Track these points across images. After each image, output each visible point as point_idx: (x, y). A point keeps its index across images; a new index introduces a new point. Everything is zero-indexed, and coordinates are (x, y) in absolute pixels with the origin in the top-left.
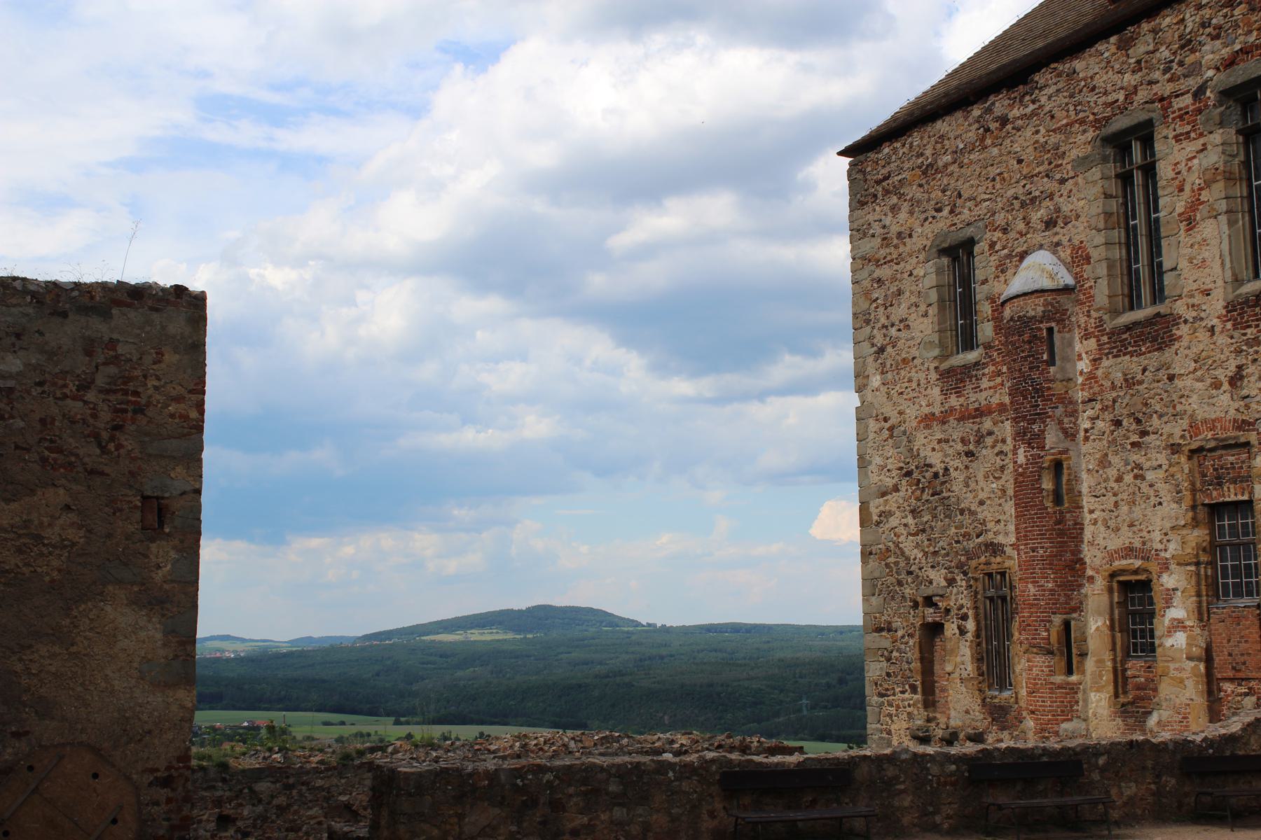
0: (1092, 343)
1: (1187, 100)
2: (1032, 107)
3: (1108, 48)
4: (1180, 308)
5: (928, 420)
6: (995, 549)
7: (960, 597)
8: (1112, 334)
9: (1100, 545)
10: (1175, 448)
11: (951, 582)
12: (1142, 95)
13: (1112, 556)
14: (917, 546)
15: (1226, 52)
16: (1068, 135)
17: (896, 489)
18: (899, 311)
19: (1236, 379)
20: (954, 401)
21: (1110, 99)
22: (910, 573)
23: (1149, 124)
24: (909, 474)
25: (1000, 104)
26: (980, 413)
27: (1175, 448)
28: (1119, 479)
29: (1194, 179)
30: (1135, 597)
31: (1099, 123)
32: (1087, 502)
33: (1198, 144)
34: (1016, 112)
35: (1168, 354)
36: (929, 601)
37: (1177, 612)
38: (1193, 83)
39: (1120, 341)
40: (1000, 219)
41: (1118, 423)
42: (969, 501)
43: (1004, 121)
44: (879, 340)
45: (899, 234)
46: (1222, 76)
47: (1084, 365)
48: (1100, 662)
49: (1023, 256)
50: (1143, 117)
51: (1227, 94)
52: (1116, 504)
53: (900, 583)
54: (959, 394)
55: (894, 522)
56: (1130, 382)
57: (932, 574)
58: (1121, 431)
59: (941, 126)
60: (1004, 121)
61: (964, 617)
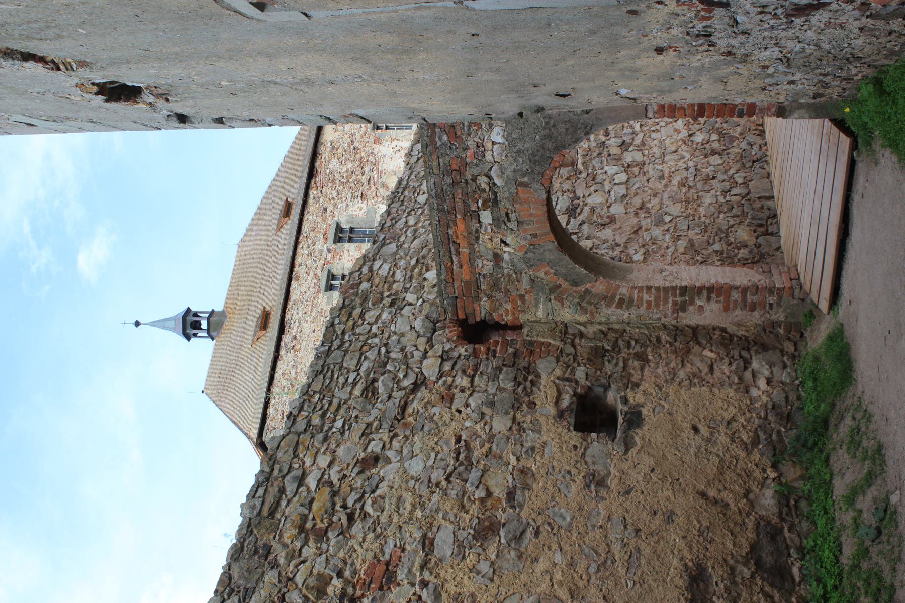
1: (329, 255)
2: (297, 324)
3: (294, 284)
12: (319, 272)
15: (322, 240)
16: (316, 306)
21: (313, 285)
23: (329, 271)
25: (286, 338)
31: (318, 292)
33: (346, 252)
34: (294, 332)
38: (326, 251)
46: (329, 241)
50: (326, 273)
51: (334, 242)
60: (295, 338)
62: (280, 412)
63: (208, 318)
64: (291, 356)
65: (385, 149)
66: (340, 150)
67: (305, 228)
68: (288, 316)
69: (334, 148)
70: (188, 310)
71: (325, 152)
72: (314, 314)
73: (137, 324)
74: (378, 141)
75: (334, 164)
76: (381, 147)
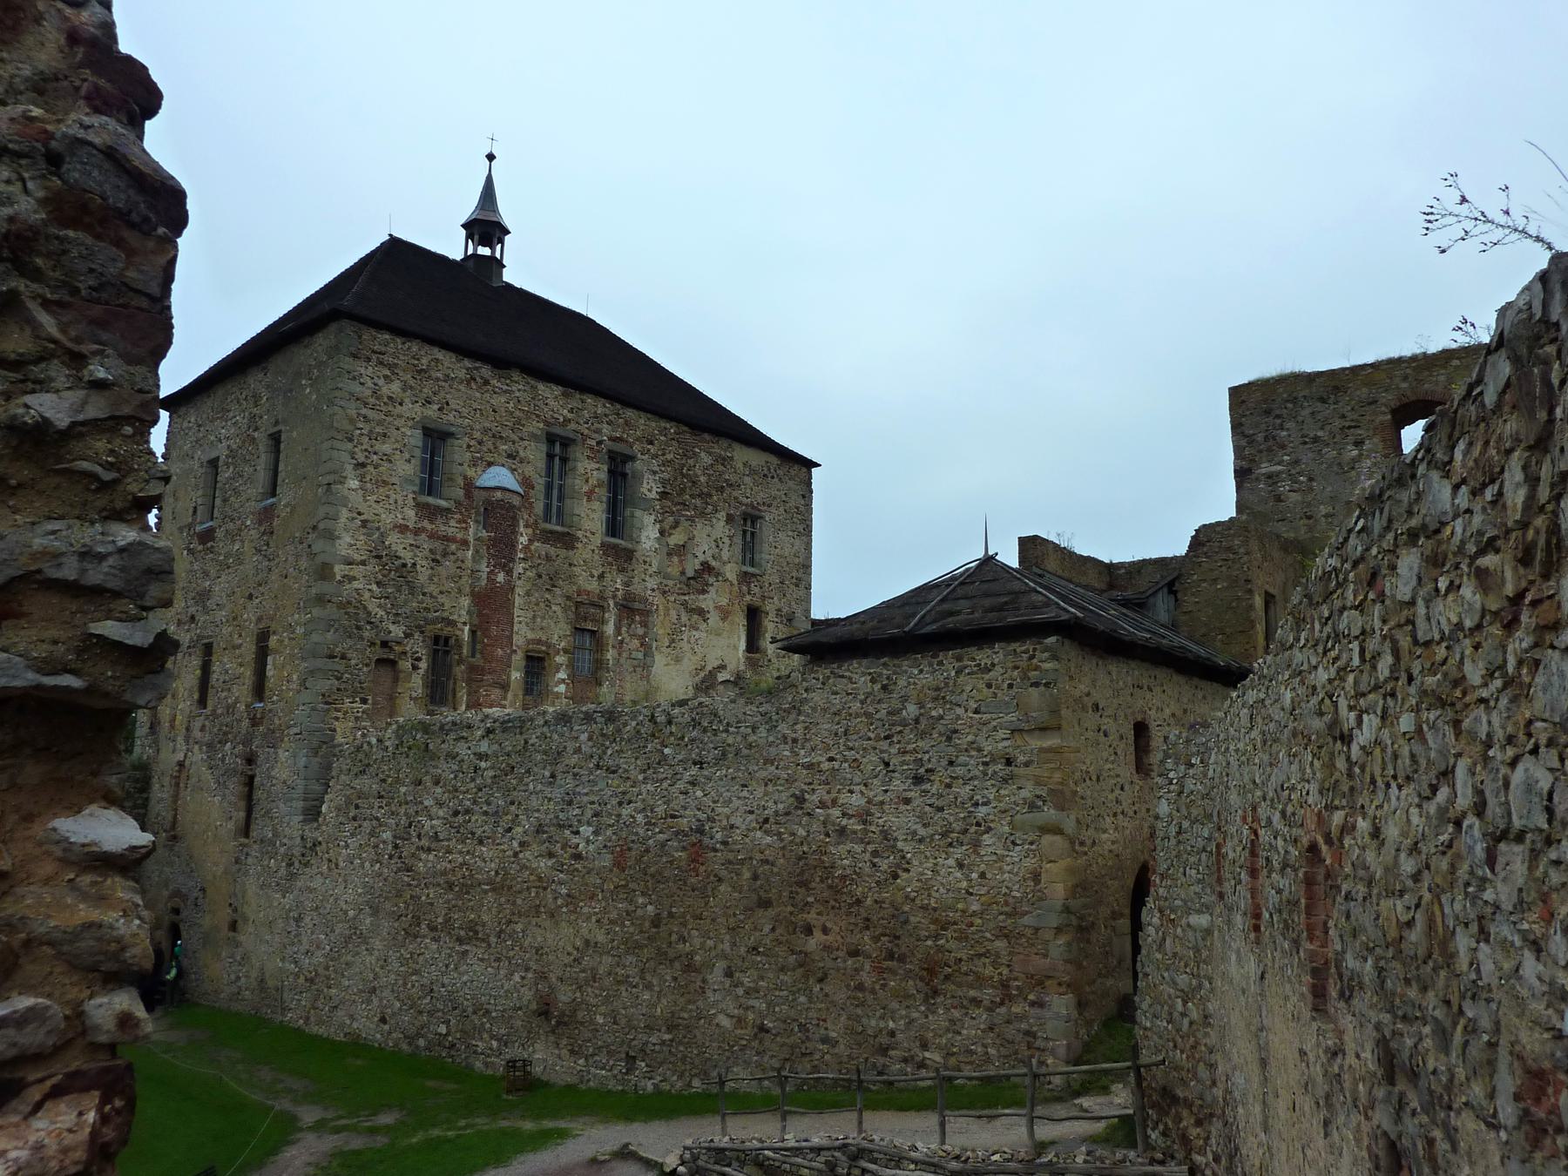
0: (530, 531)
1: (594, 443)
4: (580, 534)
5: (402, 529)
6: (452, 623)
7: (418, 646)
8: (544, 531)
9: (522, 634)
10: (568, 598)
11: (407, 636)
12: (573, 426)
13: (529, 642)
14: (380, 606)
17: (363, 563)
18: (387, 448)
19: (601, 576)
20: (426, 524)
22: (369, 623)
24: (379, 557)
25: (486, 371)
26: (446, 539)
27: (568, 598)
28: (537, 604)
29: (593, 481)
30: (536, 664)
32: (517, 612)
35: (571, 553)
36: (385, 644)
37: (562, 675)
39: (548, 537)
40: (477, 435)
41: (540, 576)
42: (432, 589)
43: (486, 382)
44: (361, 458)
45: (390, 398)
47: (523, 540)
48: (515, 695)
49: (490, 464)
52: (534, 617)
53: (358, 628)
54: (431, 522)
55: (356, 584)
56: (548, 558)
57: (392, 627)
58: (540, 582)
59: (439, 354)
60: (486, 382)
61: (419, 659)
62: (383, 349)
63: (492, 258)
64: (462, 374)
65: (720, 528)
66: (721, 468)
67: (630, 413)
68: (516, 375)
69: (724, 461)
70: (508, 232)
71: (720, 448)
72: (517, 413)
73: (491, 157)
74: (730, 519)
75: (706, 459)
76: (722, 523)
